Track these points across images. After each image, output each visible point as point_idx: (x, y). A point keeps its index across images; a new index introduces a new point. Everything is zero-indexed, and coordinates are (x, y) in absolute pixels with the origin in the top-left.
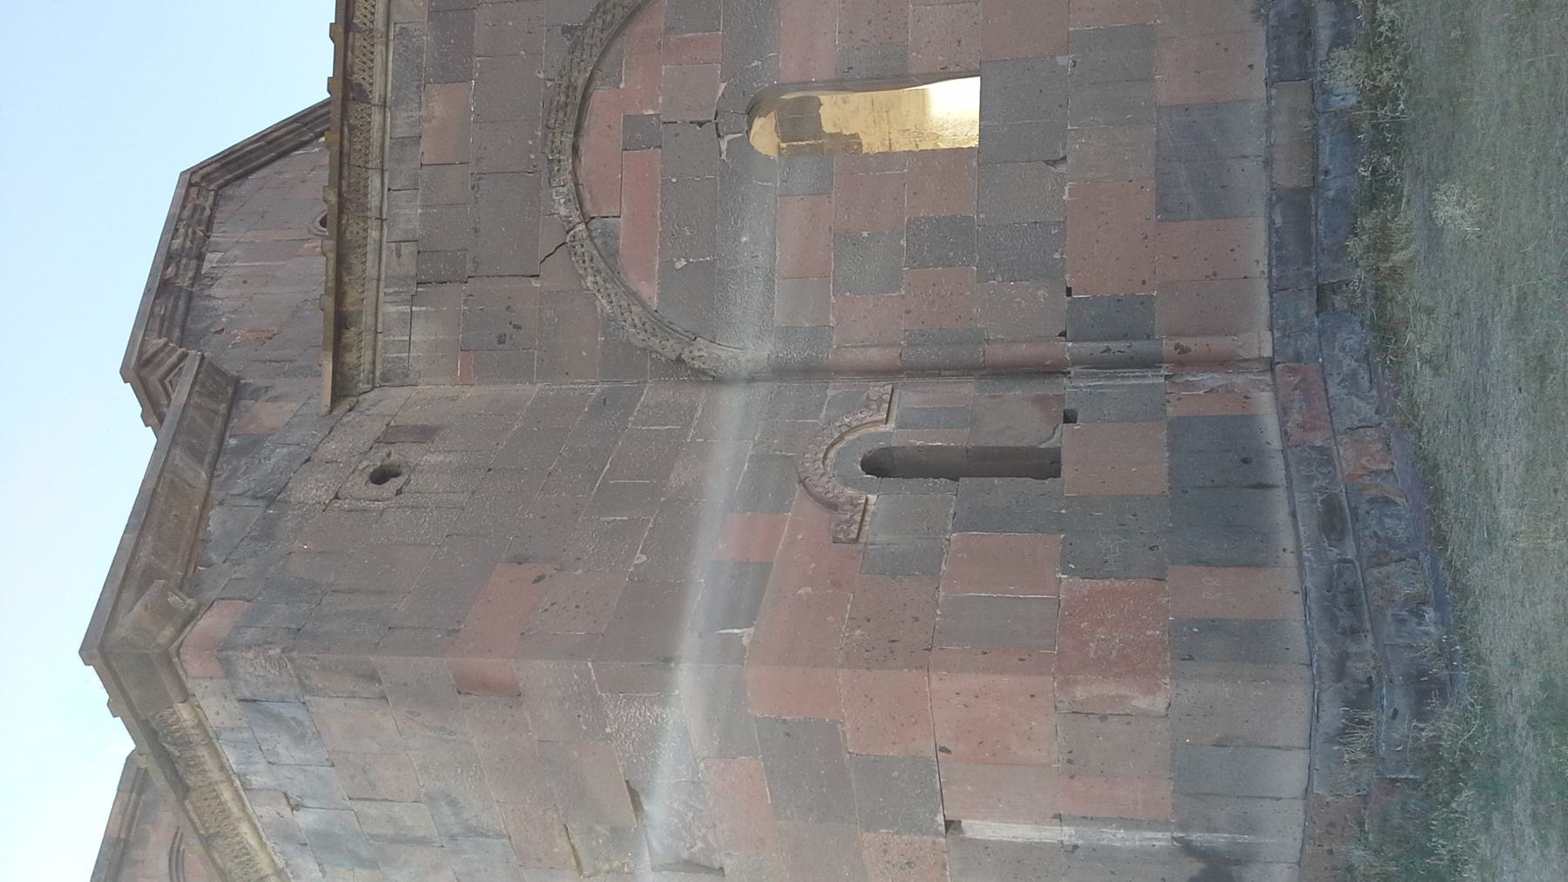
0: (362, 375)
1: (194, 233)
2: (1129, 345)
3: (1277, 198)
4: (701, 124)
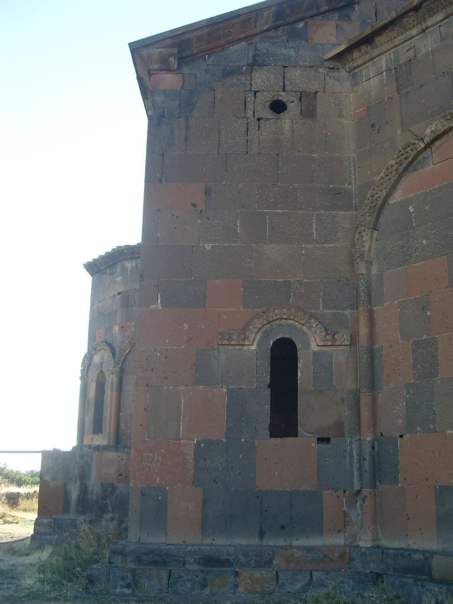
0: (351, 64)
2: (367, 471)
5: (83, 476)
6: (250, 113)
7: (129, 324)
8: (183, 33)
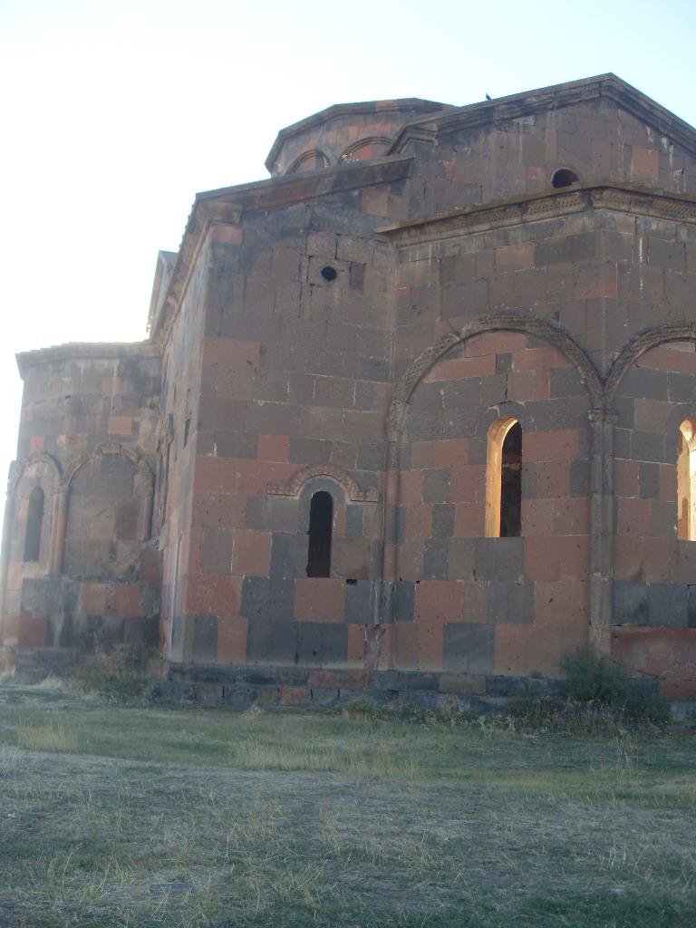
1: (551, 102)
3: (436, 676)
4: (506, 393)
5: (69, 607)
7: (79, 435)
8: (249, 190)
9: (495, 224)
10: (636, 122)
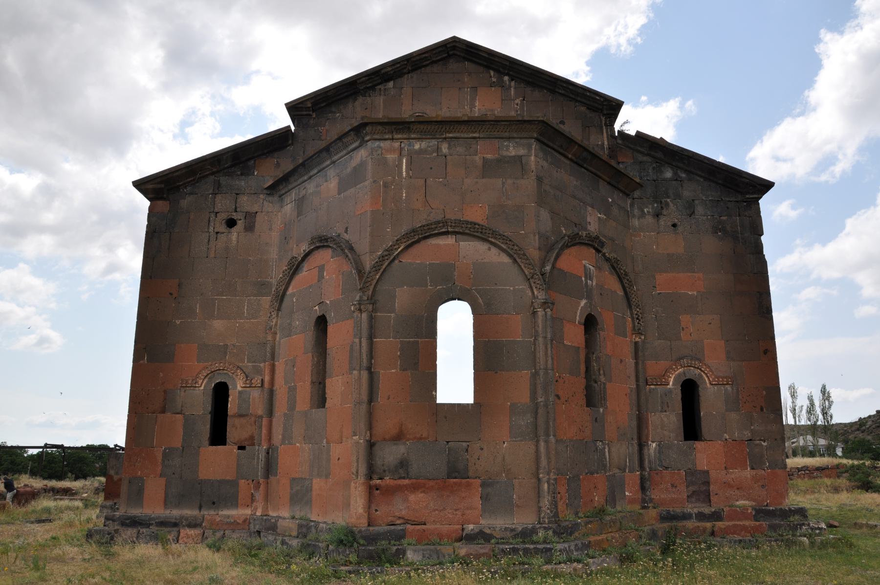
6: (211, 229)
9: (319, 168)
10: (481, 69)
